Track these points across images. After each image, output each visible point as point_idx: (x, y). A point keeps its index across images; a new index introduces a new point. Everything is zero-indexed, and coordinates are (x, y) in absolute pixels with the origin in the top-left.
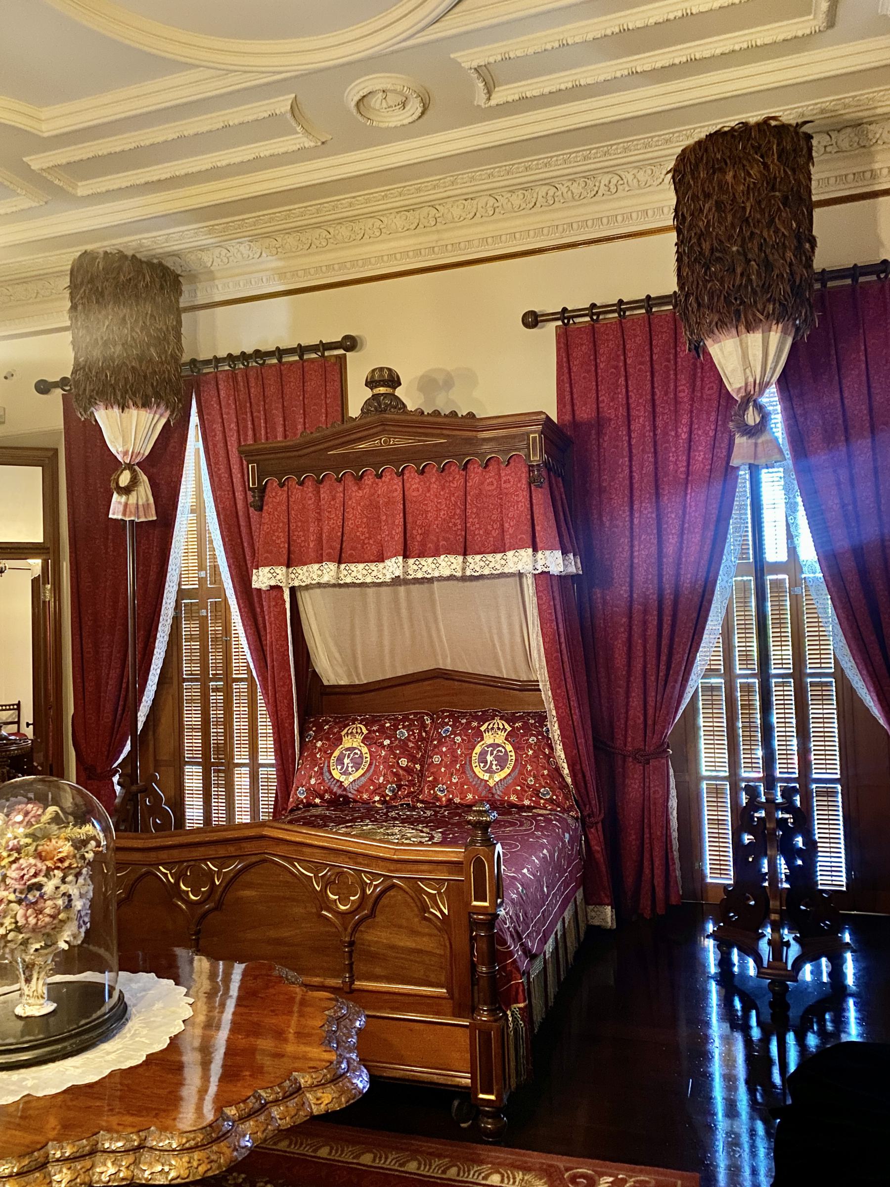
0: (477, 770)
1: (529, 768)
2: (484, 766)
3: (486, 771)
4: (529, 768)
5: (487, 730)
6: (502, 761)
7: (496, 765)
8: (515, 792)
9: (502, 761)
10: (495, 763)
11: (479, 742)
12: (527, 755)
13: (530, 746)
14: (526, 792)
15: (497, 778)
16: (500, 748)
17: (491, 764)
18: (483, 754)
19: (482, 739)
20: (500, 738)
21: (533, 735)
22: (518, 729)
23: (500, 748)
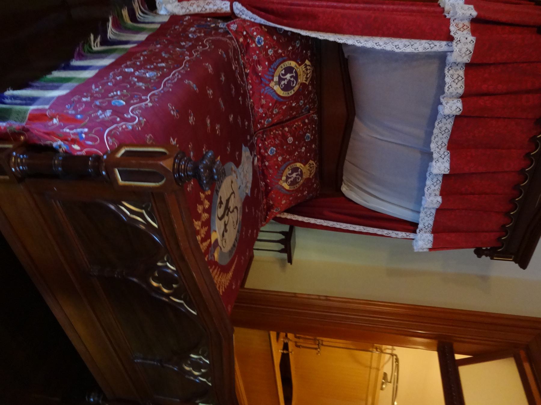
0: (279, 69)
1: (284, 107)
2: (283, 75)
3: (279, 77)
4: (284, 107)
6: (287, 88)
7: (284, 84)
8: (267, 103)
9: (287, 88)
10: (286, 82)
11: (297, 63)
12: (292, 104)
14: (268, 110)
15: (277, 88)
16: (295, 82)
17: (284, 79)
19: (300, 65)
20: (302, 79)
21: (304, 101)
23: (295, 82)
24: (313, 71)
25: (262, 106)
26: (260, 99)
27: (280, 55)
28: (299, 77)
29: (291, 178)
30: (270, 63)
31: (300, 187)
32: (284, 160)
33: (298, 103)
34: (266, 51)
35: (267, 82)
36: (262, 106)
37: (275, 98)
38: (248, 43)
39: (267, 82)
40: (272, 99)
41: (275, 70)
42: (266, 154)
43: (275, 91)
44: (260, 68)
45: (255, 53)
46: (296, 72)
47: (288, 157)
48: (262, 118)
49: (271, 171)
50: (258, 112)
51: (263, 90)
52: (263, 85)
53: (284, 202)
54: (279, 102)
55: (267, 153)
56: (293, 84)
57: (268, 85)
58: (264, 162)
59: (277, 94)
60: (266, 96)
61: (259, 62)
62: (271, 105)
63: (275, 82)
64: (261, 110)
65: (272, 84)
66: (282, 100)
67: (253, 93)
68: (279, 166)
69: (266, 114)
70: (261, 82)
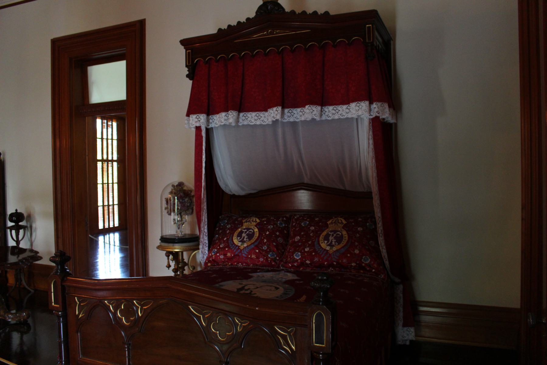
1: (265, 241)
4: (265, 241)
5: (246, 222)
8: (255, 253)
12: (266, 234)
13: (268, 230)
14: (261, 253)
18: (241, 232)
19: (242, 226)
22: (264, 221)
24: (255, 217)
25: (258, 258)
26: (251, 258)
27: (228, 239)
28: (250, 227)
29: (332, 242)
30: (228, 247)
31: (348, 234)
32: (312, 246)
33: (268, 230)
34: (220, 248)
35: (239, 251)
36: (258, 258)
37: (253, 246)
38: (213, 260)
39: (239, 251)
40: (253, 249)
41: (234, 243)
42: (299, 261)
43: (247, 246)
44: (229, 254)
45: (219, 256)
46: (331, 231)
47: (310, 243)
48: (267, 260)
49: (316, 259)
50: (262, 262)
51: (244, 255)
52: (240, 254)
53: (357, 251)
54: (259, 244)
55: (297, 260)
56: (251, 232)
57: (241, 250)
58: (307, 264)
59: (250, 245)
60: (250, 253)
61: (225, 255)
62: (257, 251)
63: (241, 245)
64: (261, 259)
65: (242, 248)
66: (258, 242)
67: (246, 263)
68: (315, 251)
69: (265, 256)
70: (238, 255)
